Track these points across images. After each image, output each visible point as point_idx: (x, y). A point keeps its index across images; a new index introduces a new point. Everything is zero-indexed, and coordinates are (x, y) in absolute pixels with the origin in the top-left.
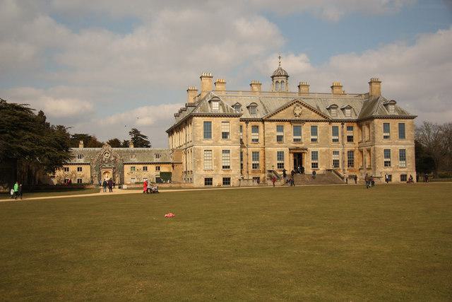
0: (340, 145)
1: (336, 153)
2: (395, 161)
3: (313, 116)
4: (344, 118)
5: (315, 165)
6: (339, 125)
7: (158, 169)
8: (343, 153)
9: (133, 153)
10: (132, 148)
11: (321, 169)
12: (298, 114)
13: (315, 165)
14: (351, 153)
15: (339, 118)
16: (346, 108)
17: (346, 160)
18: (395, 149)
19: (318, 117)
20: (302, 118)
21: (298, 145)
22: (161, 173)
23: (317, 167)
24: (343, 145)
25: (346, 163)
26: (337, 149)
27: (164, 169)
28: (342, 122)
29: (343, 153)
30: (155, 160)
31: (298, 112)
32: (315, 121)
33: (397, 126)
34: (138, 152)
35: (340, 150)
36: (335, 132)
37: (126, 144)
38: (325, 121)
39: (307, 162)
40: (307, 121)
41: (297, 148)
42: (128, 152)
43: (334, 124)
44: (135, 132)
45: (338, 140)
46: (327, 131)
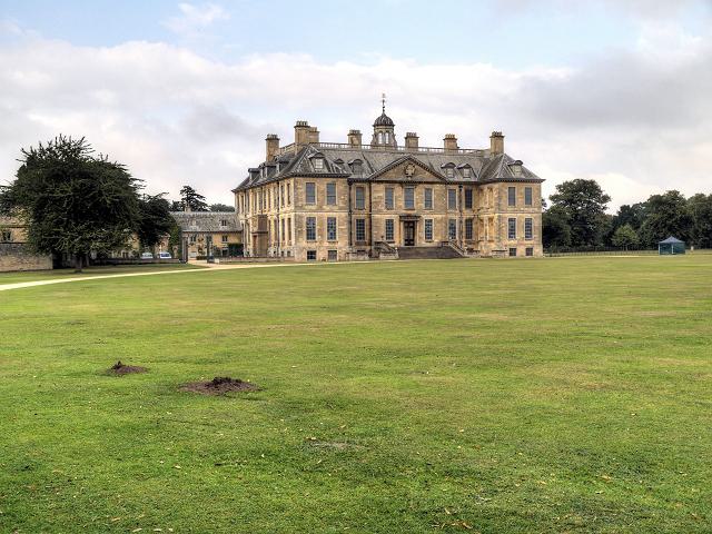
2: (520, 234)
3: (427, 176)
4: (461, 179)
5: (429, 235)
6: (456, 187)
7: (225, 239)
8: (461, 222)
9: (193, 217)
10: (189, 212)
11: (436, 240)
12: (410, 174)
13: (429, 235)
14: (469, 222)
15: (456, 179)
17: (464, 230)
18: (521, 217)
19: (432, 179)
21: (409, 212)
22: (231, 246)
25: (464, 234)
27: (233, 240)
28: (460, 184)
30: (221, 228)
31: (410, 172)
33: (523, 191)
34: (198, 216)
37: (176, 207)
39: (421, 230)
41: (409, 216)
42: (184, 216)
43: (452, 187)
44: (188, 190)
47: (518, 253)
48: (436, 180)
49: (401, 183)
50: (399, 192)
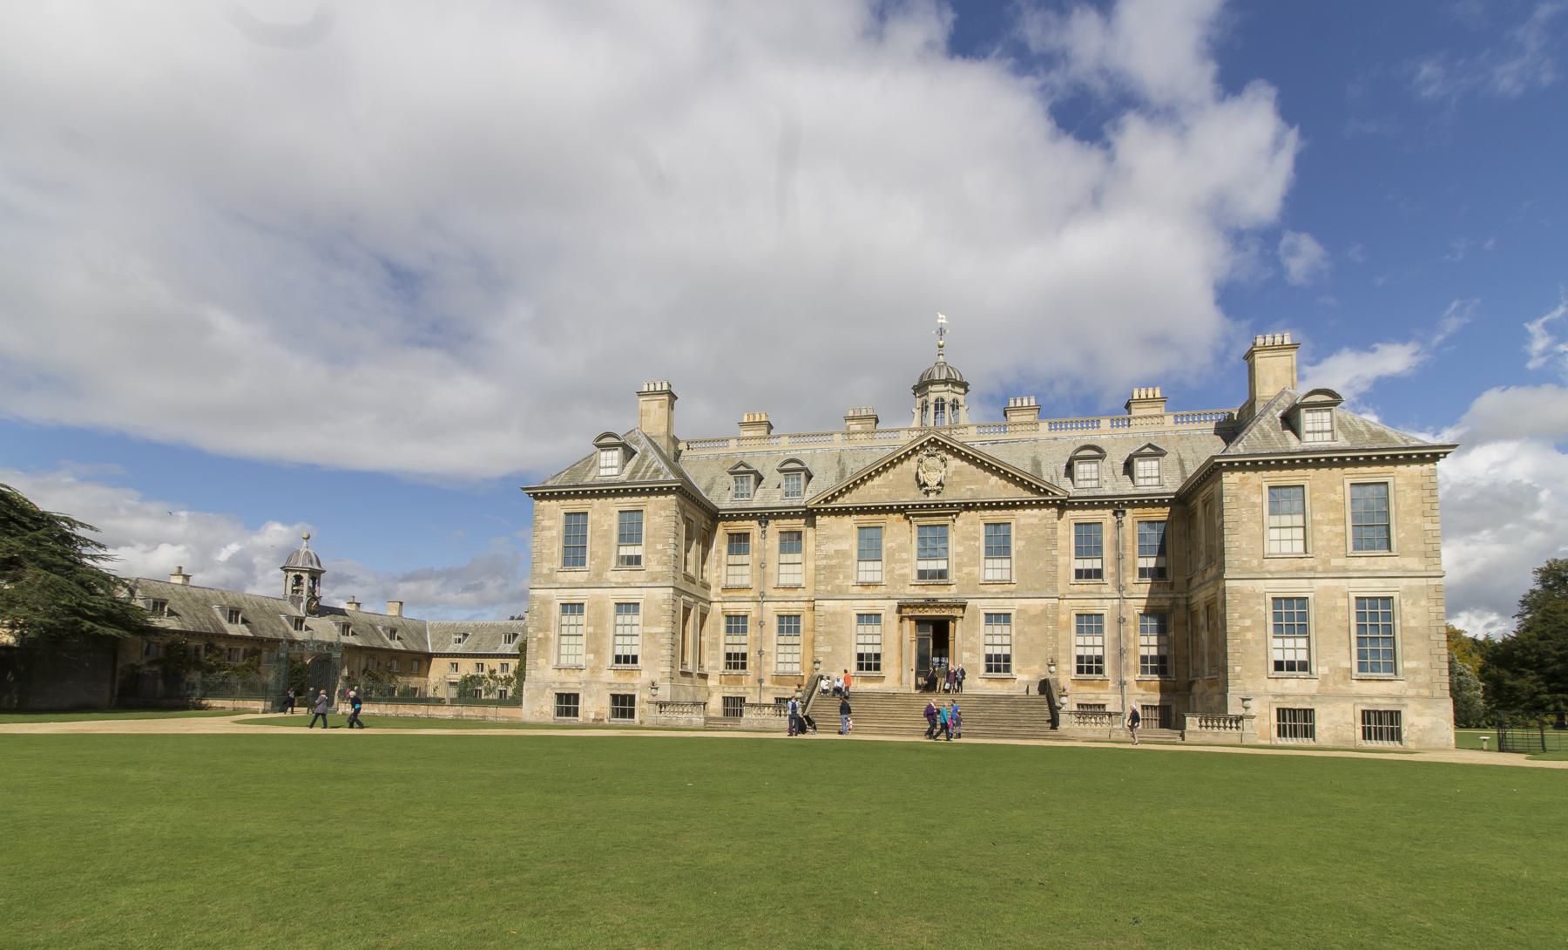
0: (1108, 589)
1: (1089, 622)
6: (1106, 517)
8: (1121, 621)
12: (932, 484)
16: (1140, 455)
20: (949, 496)
21: (933, 593)
23: (1007, 669)
24: (1120, 588)
26: (1094, 606)
29: (1121, 621)
31: (932, 479)
32: (997, 506)
35: (1107, 608)
36: (1088, 542)
38: (1038, 505)
40: (968, 507)
41: (930, 603)
45: (1098, 573)
46: (1051, 540)
47: (1321, 724)
48: (1027, 495)
49: (902, 510)
50: (899, 535)
